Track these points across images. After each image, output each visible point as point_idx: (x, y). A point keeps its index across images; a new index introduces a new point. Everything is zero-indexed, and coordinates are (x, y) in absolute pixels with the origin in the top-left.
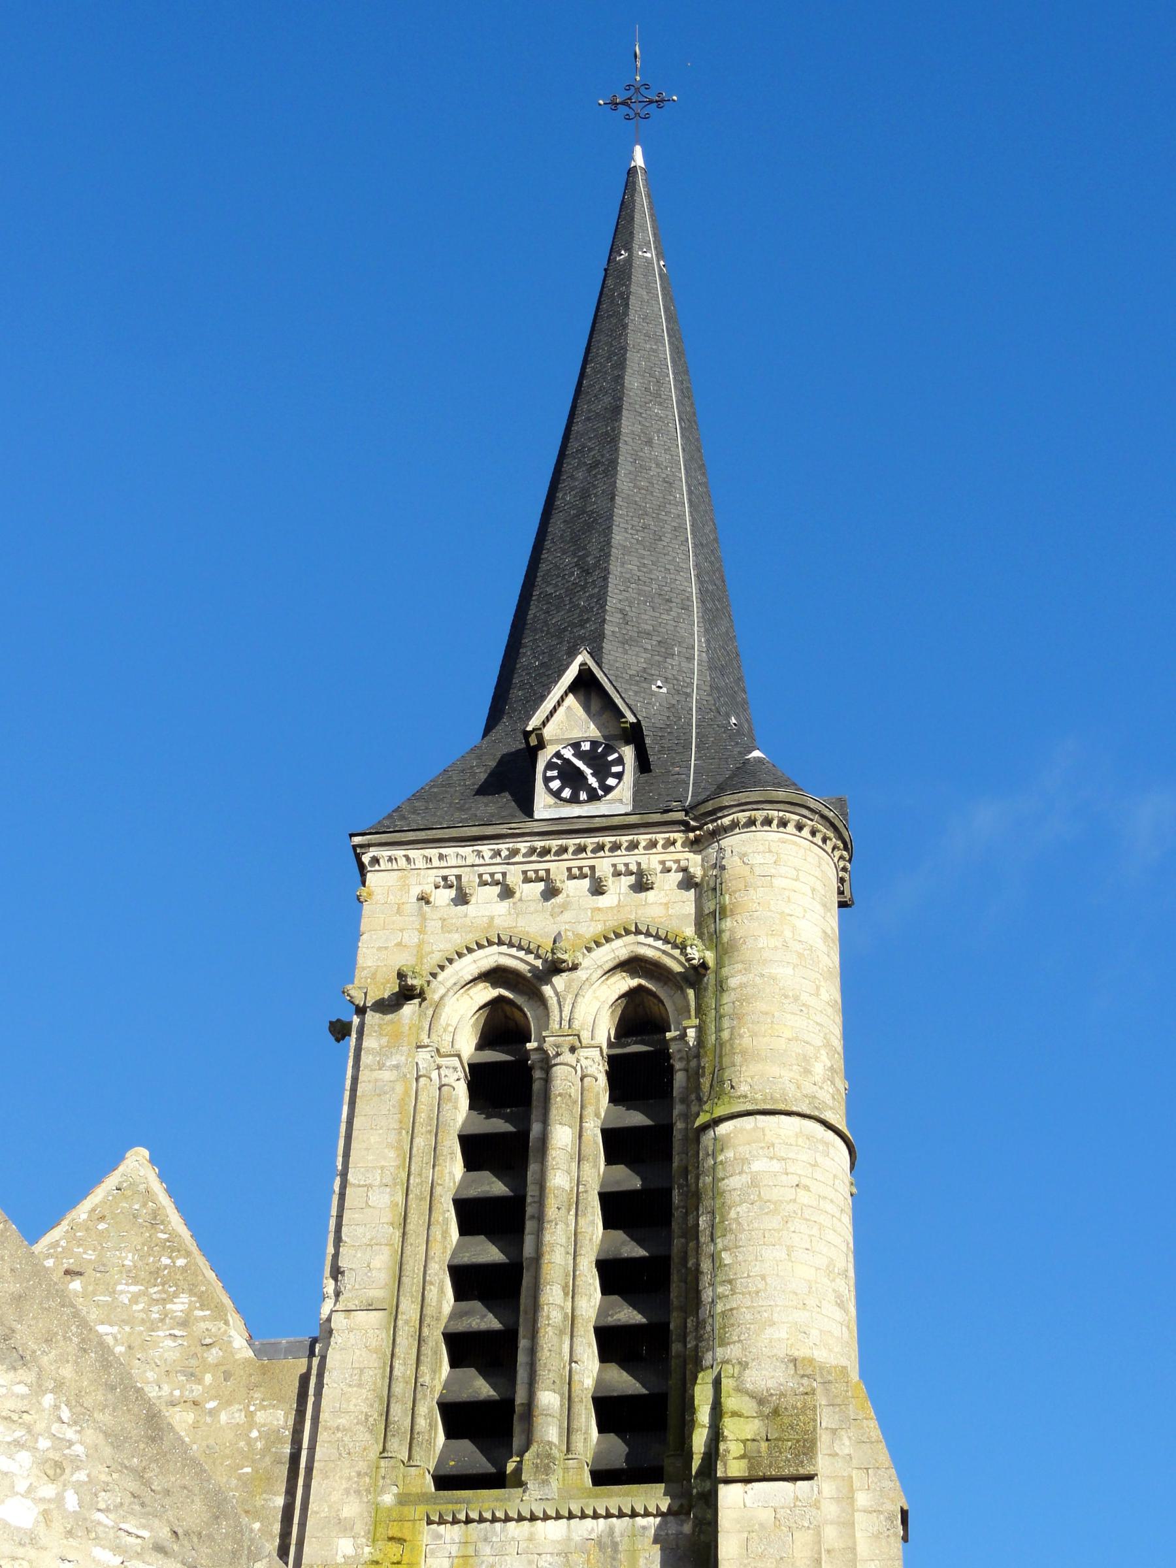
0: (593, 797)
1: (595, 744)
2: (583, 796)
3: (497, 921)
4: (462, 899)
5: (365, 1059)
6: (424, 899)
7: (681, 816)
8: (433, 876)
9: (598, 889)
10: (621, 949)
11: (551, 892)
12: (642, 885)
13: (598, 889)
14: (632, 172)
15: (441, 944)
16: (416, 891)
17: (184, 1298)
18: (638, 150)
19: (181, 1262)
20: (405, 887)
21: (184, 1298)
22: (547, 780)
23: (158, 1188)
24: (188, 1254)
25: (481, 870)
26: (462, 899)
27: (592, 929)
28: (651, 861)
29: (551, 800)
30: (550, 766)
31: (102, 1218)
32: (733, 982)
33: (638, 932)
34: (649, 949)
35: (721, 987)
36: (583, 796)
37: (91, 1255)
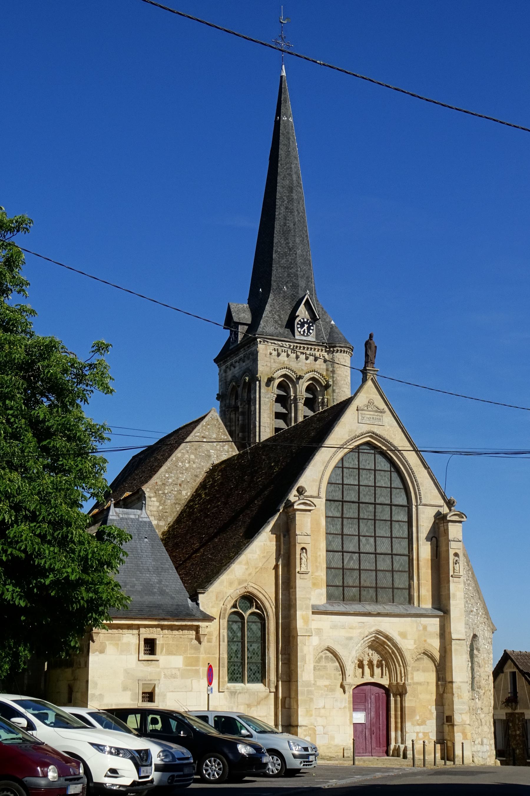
0: (307, 335)
1: (308, 320)
2: (305, 334)
3: (286, 362)
4: (279, 355)
5: (262, 395)
6: (271, 354)
7: (325, 344)
8: (272, 348)
9: (307, 359)
10: (310, 375)
11: (297, 357)
12: (316, 359)
13: (307, 359)
14: (282, 77)
15: (275, 366)
16: (269, 351)
18: (283, 66)
20: (266, 349)
22: (298, 328)
24: (227, 436)
25: (283, 348)
26: (279, 355)
27: (305, 369)
28: (317, 354)
29: (299, 334)
30: (298, 324)
31: (208, 425)
32: (337, 391)
33: (315, 372)
34: (317, 376)
35: (334, 391)
36: (305, 334)
37: (207, 433)
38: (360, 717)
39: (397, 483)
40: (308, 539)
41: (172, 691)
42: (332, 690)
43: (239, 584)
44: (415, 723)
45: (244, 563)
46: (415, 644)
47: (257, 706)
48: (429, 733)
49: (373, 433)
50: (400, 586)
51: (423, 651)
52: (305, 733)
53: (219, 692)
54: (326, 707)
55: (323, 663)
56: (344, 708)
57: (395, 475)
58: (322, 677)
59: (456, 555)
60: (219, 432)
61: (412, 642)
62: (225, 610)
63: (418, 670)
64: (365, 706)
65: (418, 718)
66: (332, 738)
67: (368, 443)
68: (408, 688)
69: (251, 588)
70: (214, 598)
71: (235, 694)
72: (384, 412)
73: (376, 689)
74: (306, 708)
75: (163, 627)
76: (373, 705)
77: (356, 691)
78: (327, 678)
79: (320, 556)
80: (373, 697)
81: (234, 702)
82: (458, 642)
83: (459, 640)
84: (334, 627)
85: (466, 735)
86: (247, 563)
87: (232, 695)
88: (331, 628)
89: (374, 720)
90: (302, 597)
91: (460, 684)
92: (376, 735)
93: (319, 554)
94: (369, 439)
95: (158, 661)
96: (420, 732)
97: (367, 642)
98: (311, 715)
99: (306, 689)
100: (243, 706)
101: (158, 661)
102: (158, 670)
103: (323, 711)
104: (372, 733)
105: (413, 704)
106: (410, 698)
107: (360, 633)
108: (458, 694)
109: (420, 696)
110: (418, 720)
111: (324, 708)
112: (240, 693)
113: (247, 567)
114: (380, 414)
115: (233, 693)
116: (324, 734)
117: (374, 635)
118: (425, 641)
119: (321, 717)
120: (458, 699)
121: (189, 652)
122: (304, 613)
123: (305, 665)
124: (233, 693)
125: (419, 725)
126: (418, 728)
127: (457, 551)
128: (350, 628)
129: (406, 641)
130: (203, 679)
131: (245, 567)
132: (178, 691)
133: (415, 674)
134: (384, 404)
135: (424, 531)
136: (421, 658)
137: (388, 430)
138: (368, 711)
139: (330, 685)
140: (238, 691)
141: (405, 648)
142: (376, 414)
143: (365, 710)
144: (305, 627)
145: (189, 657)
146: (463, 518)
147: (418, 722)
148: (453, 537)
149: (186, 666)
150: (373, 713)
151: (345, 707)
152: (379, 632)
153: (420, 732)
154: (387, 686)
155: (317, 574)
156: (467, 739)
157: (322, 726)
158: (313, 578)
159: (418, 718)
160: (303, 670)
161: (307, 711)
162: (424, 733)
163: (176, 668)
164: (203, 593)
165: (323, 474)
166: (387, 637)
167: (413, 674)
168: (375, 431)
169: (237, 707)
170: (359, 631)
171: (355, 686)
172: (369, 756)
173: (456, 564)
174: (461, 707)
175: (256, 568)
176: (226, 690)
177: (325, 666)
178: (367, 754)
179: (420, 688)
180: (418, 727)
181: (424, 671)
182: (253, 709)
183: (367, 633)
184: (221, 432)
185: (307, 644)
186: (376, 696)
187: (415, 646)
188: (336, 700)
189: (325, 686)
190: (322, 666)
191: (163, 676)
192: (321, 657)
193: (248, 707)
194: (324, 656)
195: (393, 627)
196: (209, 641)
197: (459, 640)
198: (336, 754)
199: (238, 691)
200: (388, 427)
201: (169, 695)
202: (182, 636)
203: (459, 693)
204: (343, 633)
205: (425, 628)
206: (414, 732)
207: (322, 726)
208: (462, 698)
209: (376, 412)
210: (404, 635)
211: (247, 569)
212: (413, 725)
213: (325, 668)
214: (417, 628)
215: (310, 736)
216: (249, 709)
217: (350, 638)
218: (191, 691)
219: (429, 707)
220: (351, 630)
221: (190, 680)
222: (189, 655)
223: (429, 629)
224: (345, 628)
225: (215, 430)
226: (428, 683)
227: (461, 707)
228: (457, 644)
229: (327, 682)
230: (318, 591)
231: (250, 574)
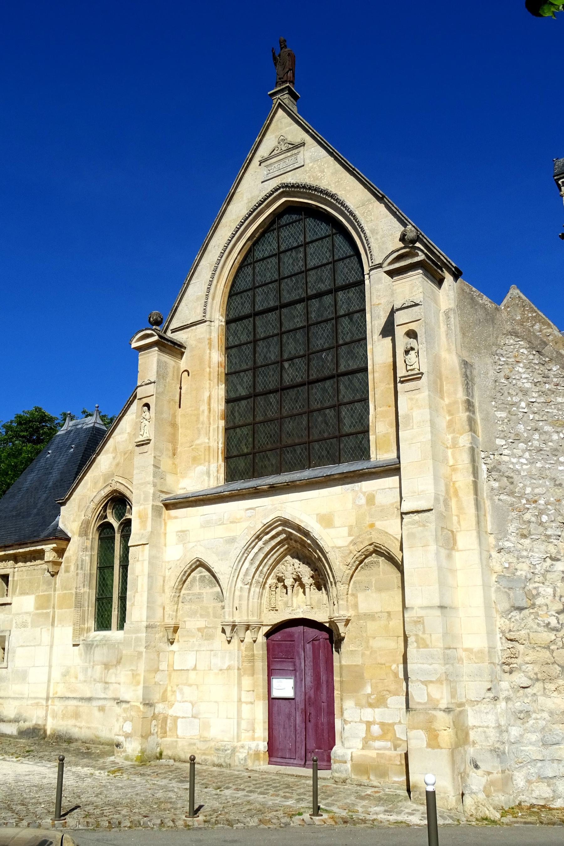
17: (538, 324)
19: (534, 314)
21: (538, 324)
23: (521, 295)
24: (536, 312)
31: (508, 307)
38: (284, 687)
39: (344, 249)
40: (151, 389)
41: (22, 646)
42: (209, 637)
43: (105, 482)
44: (364, 702)
45: (111, 450)
46: (350, 535)
47: (116, 666)
48: (393, 724)
49: (287, 186)
50: (353, 430)
51: (371, 548)
52: (125, 715)
53: (74, 645)
54: (197, 668)
55: (197, 589)
56: (227, 669)
57: (339, 240)
58: (193, 614)
59: (411, 334)
60: (524, 311)
61: (345, 531)
62: (86, 523)
63: (367, 588)
64: (295, 665)
65: (368, 690)
66: (206, 726)
67: (288, 209)
68: (342, 629)
69: (118, 484)
70: (76, 508)
71: (91, 648)
72: (303, 144)
73: (312, 632)
74: (132, 670)
75: (16, 558)
76: (309, 663)
77: (277, 636)
78: (201, 616)
79: (203, 412)
80: (308, 646)
81: (90, 661)
82: (416, 517)
83: (418, 512)
84: (207, 525)
85: (437, 736)
86: (115, 449)
87: (87, 649)
88: (202, 527)
89: (312, 693)
90: (140, 481)
91: (422, 613)
92: (316, 725)
93: (201, 409)
94: (284, 200)
95: (10, 604)
96: (373, 723)
97: (273, 543)
98: (138, 683)
99: (134, 636)
100: (99, 666)
101: (10, 604)
102: (11, 616)
103: (192, 674)
104: (306, 720)
105: (358, 661)
106: (352, 648)
107: (248, 528)
108: (417, 635)
109: (372, 643)
110: (369, 696)
111: (195, 669)
112: (97, 646)
113: (114, 455)
114: (295, 151)
115: (90, 646)
116: (193, 717)
117: (280, 528)
118: (372, 526)
119: (190, 685)
120: (418, 647)
121: (41, 588)
122: (142, 507)
123: (137, 595)
124: (90, 646)
125: (371, 705)
126: (368, 714)
127: (412, 326)
128: (231, 522)
129: (332, 531)
130: (57, 626)
131: (111, 456)
132: (27, 646)
133: (361, 597)
134: (303, 132)
135: (382, 313)
136: (372, 563)
137: (312, 167)
138: (300, 674)
139: (206, 627)
140: (95, 643)
141: (331, 544)
142: (289, 154)
143: (294, 672)
144: (142, 531)
145: (41, 596)
146: (417, 255)
147: (370, 701)
148: (403, 302)
149: (37, 609)
150: (309, 679)
151: (229, 668)
152: (285, 523)
153: (373, 723)
154: (327, 625)
155: (198, 442)
156: (439, 747)
157: (191, 702)
158: (193, 450)
159: (368, 690)
160: (133, 604)
161: (133, 674)
162: (382, 725)
163: (26, 613)
164: (64, 504)
165: (217, 282)
166: (299, 529)
167: (357, 597)
168: (290, 179)
169: (93, 667)
170: (245, 525)
171: (269, 628)
172: (300, 766)
173: (407, 352)
174: (426, 666)
175: (125, 454)
176: (81, 643)
177: (200, 594)
178: (295, 762)
179: (371, 626)
180: (369, 710)
181: (379, 590)
182: (111, 671)
183: (259, 527)
184: (527, 310)
185: (140, 559)
186: (313, 645)
187: (352, 538)
188: (215, 655)
189: (199, 630)
190: (194, 594)
191: (14, 625)
192: (194, 578)
193: (105, 668)
194: (198, 576)
195: (306, 507)
196: (67, 571)
197: (418, 512)
198: (203, 757)
199: (95, 643)
200: (311, 165)
201: (19, 651)
202: (36, 568)
203: (420, 634)
204: (221, 532)
205: (371, 499)
206: (361, 721)
207: (191, 702)
208: (426, 646)
209: (288, 150)
210: (327, 521)
211: (114, 458)
212: (359, 705)
213: (199, 596)
214: (354, 503)
215: (132, 721)
216: (106, 671)
217: (232, 540)
218: (39, 645)
219: (394, 667)
220: (233, 525)
221: (39, 629)
222: (41, 594)
223: (380, 499)
224: (223, 524)
225: (519, 311)
226: (389, 613)
227: (426, 666)
228: (413, 523)
229: (201, 623)
230: (202, 468)
231: (118, 465)
